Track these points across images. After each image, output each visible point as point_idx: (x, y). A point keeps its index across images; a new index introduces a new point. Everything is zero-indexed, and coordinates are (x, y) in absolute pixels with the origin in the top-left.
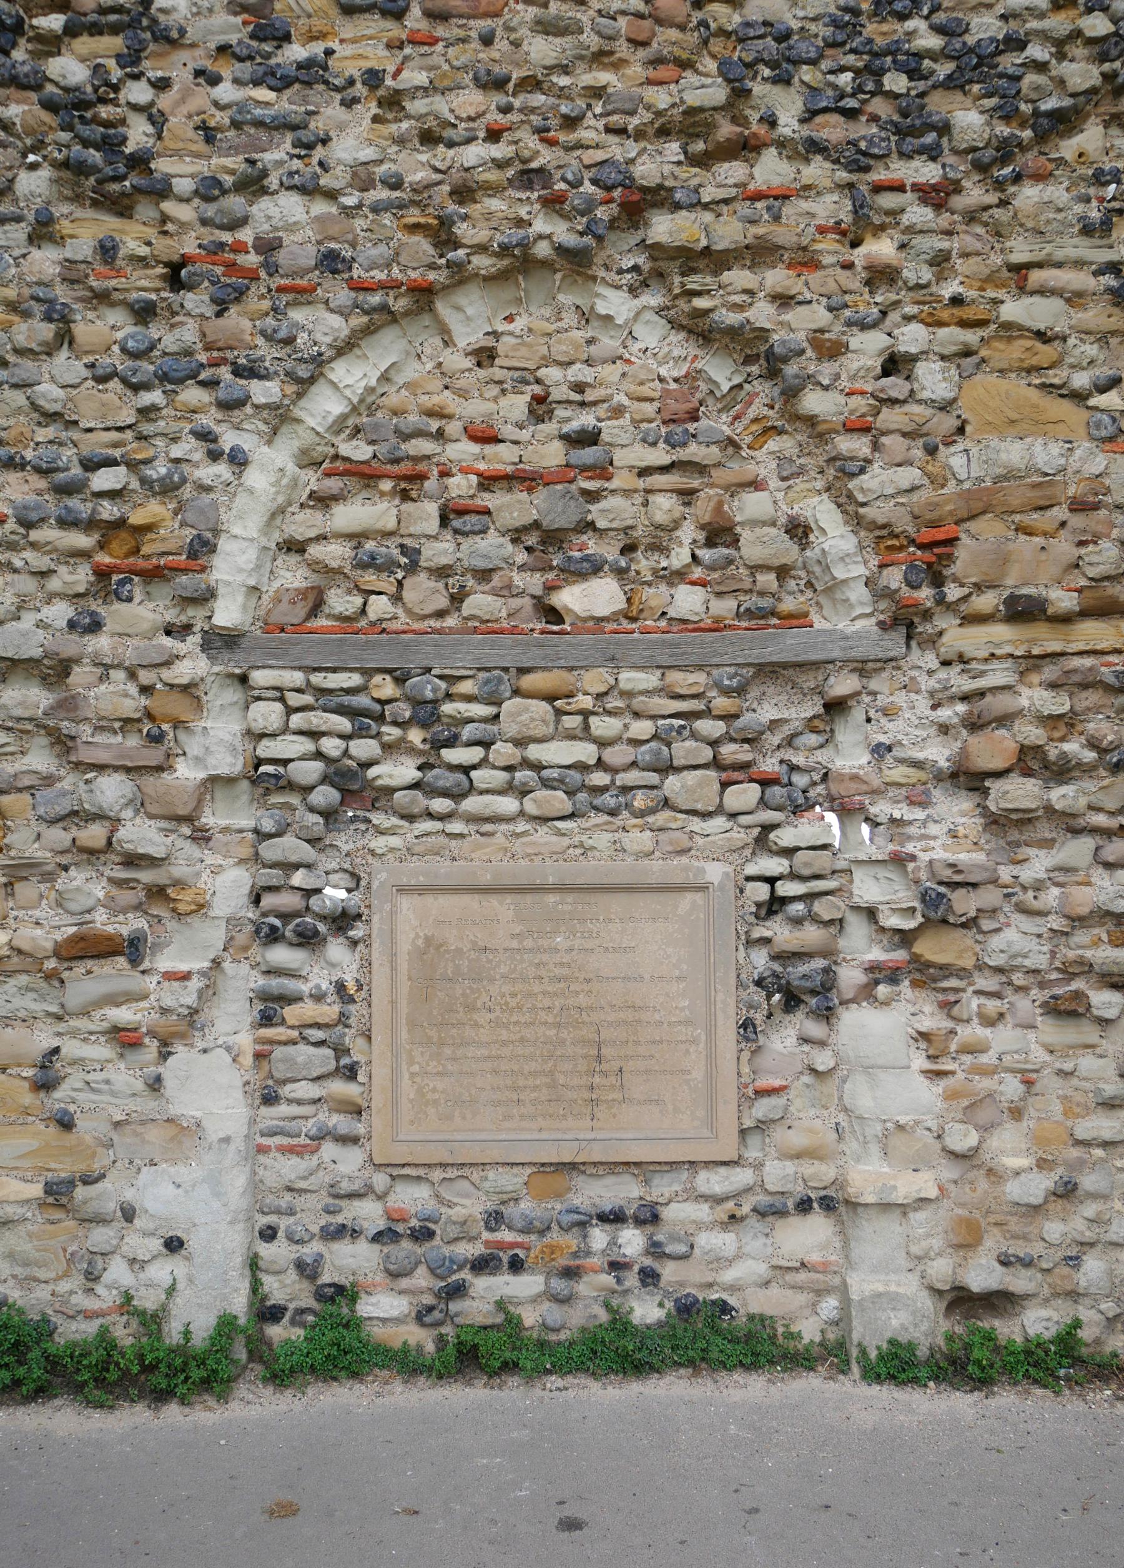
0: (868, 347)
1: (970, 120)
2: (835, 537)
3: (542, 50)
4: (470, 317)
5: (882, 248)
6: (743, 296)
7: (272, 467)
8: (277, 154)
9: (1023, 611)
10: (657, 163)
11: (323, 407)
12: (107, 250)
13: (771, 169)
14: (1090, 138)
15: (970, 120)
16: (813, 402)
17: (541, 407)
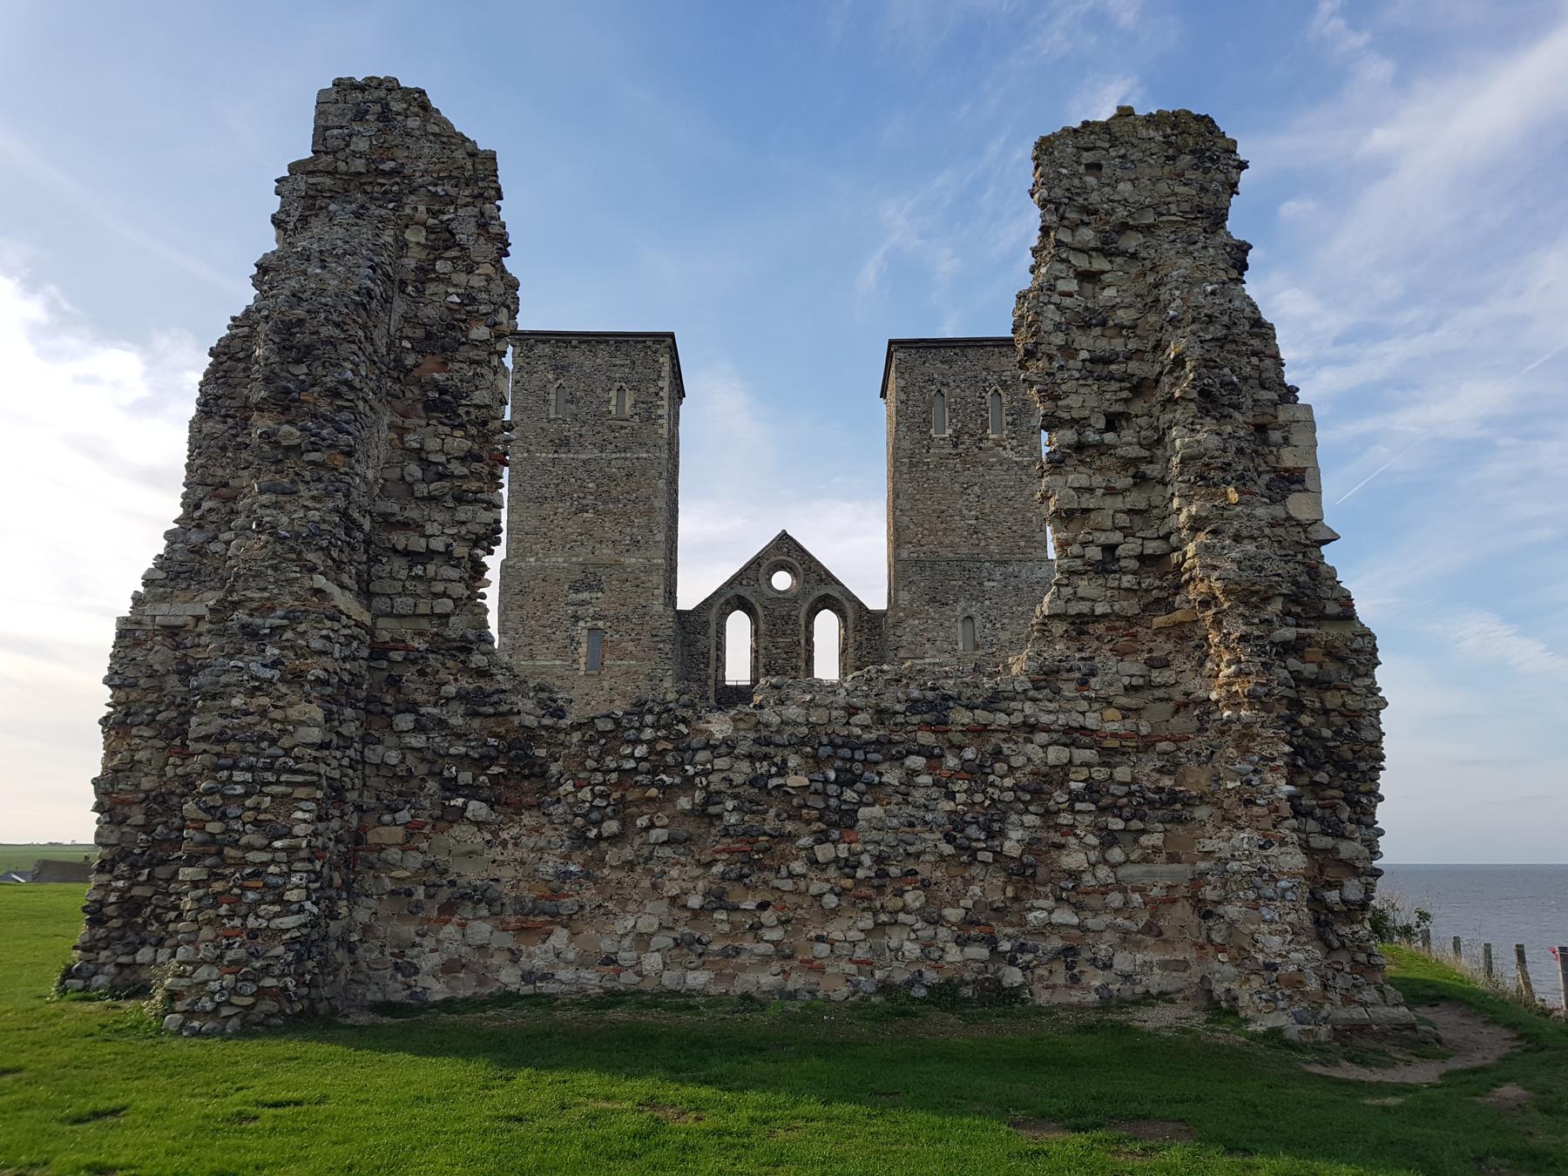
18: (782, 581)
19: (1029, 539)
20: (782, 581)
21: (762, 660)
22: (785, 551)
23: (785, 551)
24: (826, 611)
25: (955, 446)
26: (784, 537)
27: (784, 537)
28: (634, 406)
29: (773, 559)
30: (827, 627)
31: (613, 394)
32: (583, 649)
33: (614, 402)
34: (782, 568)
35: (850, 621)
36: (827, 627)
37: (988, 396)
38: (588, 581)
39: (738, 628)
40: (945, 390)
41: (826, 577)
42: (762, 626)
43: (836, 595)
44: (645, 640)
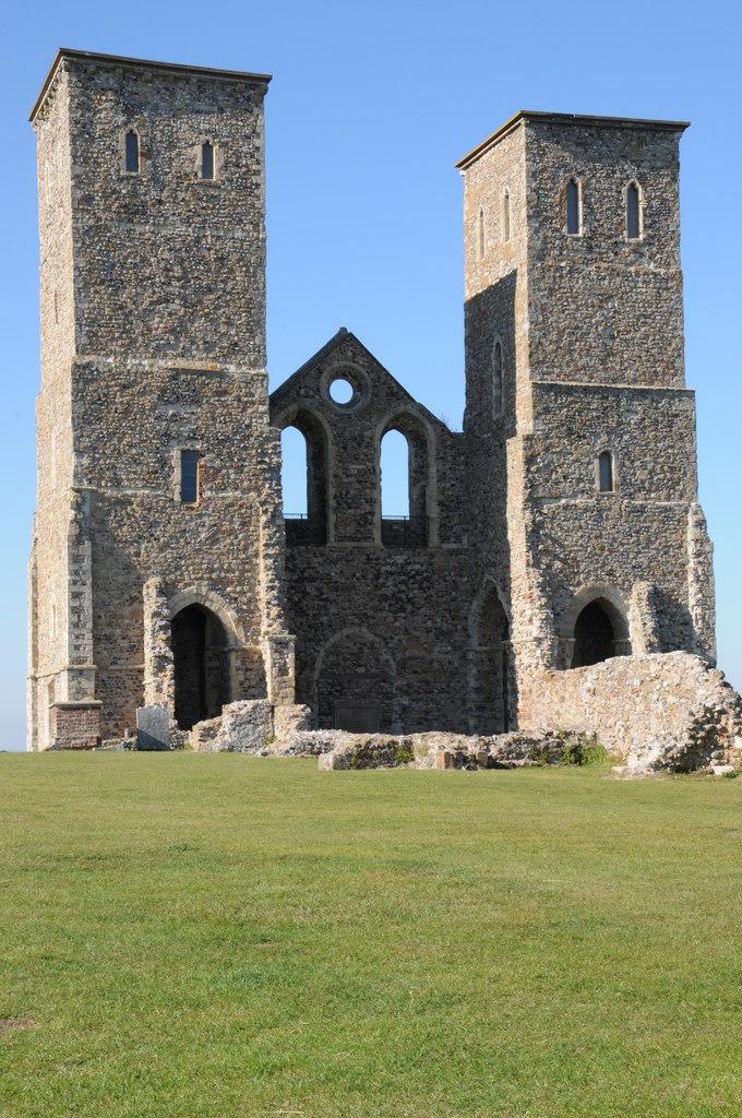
0: (396, 638)
1: (409, 608)
2: (392, 662)
3: (356, 597)
4: (346, 632)
5: (398, 624)
6: (382, 630)
7: (322, 653)
8: (323, 612)
9: (415, 672)
10: (370, 613)
11: (328, 645)
12: (301, 623)
13: (385, 614)
14: (423, 610)
15: (409, 608)
16: (391, 645)
17: (355, 644)
18: (341, 392)
19: (670, 365)
20: (341, 392)
21: (332, 491)
22: (345, 354)
23: (345, 354)
24: (394, 432)
25: (590, 249)
26: (345, 342)
27: (345, 342)
28: (226, 166)
29: (336, 364)
30: (394, 452)
31: (198, 150)
32: (177, 476)
33: (199, 162)
34: (344, 376)
35: (432, 449)
36: (394, 452)
37: (624, 190)
38: (181, 389)
39: (293, 444)
40: (579, 181)
41: (397, 393)
42: (332, 450)
43: (414, 412)
44: (251, 466)
